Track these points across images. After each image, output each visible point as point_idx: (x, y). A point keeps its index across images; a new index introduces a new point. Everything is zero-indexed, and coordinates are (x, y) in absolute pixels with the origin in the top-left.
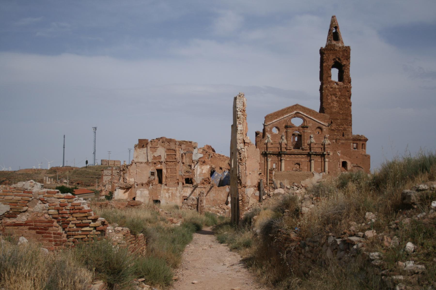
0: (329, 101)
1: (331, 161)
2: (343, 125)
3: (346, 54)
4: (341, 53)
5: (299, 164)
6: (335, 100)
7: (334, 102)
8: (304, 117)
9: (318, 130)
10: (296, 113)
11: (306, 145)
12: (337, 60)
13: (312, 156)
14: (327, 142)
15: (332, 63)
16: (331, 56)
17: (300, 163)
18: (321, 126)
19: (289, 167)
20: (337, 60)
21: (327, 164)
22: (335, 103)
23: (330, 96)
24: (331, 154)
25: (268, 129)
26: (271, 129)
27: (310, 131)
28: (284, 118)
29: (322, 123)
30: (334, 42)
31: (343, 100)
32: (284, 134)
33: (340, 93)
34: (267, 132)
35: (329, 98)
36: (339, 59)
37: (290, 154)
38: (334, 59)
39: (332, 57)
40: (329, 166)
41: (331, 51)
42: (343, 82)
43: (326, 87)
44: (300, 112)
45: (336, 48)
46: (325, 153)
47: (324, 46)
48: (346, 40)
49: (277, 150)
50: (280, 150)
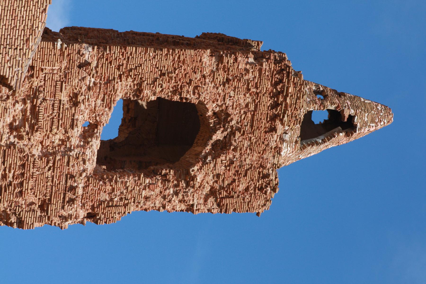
12: (218, 136)
20: (218, 136)
33: (37, 152)
36: (222, 147)
38: (222, 117)
39: (238, 100)
41: (267, 101)
42: (97, 175)
43: (85, 65)
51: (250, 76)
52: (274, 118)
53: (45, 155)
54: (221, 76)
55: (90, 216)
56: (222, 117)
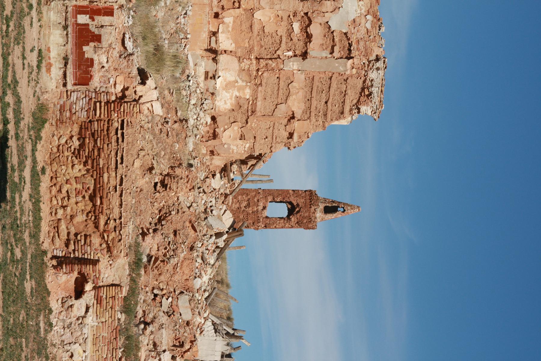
0: (240, 197)
3: (305, 221)
4: (307, 214)
6: (242, 206)
7: (238, 203)
12: (297, 209)
16: (303, 200)
20: (297, 209)
22: (237, 205)
23: (247, 199)
30: (322, 206)
31: (241, 217)
33: (251, 212)
35: (244, 196)
36: (298, 212)
38: (298, 205)
45: (313, 208)
51: (303, 195)
52: (310, 205)
53: (253, 212)
54: (295, 195)
55: (265, 226)
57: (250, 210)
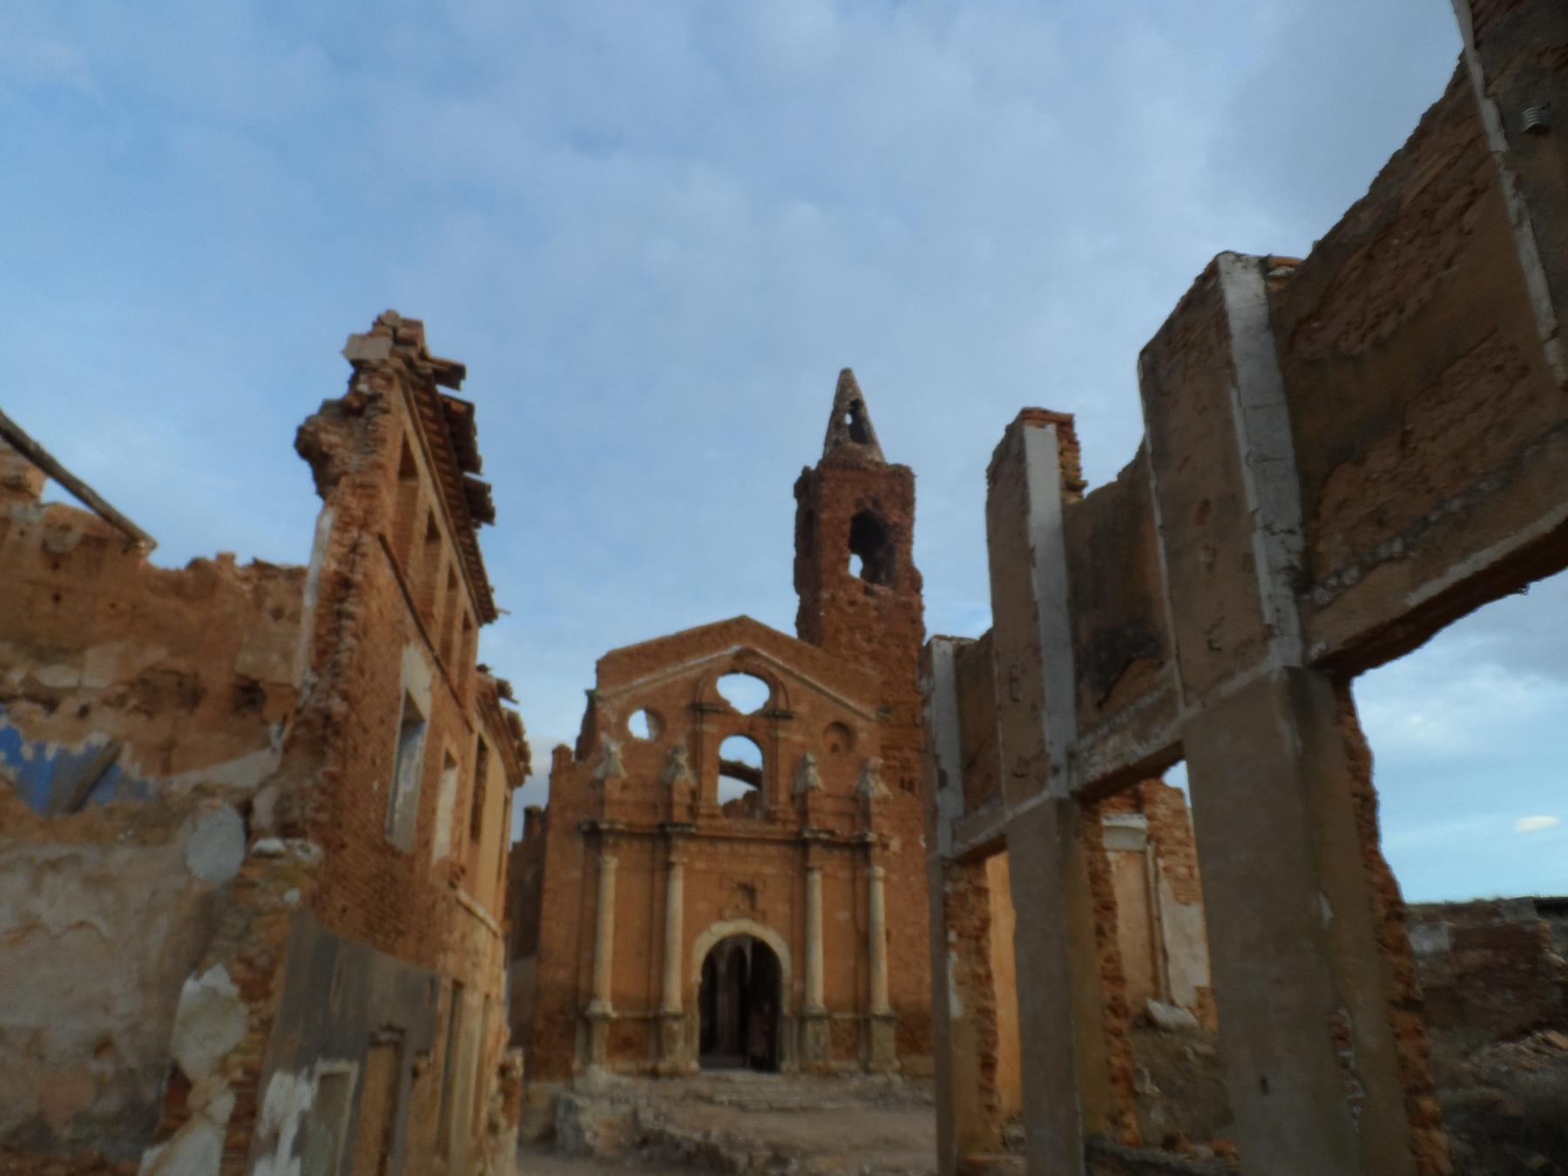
1: (895, 878)
2: (899, 749)
5: (749, 891)
8: (774, 670)
9: (834, 737)
10: (738, 656)
11: (783, 797)
12: (869, 505)
13: (815, 850)
14: (879, 788)
15: (847, 511)
17: (758, 885)
18: (847, 717)
19: (702, 906)
21: (879, 890)
24: (895, 845)
25: (608, 713)
26: (624, 715)
27: (798, 738)
28: (685, 670)
29: (851, 703)
32: (681, 741)
34: (606, 728)
36: (876, 502)
37: (713, 839)
38: (859, 503)
40: (887, 902)
42: (894, 588)
44: (759, 650)
46: (872, 837)
47: (813, 465)
48: (892, 447)
49: (645, 819)
50: (661, 819)
56: (859, 503)
57: (879, 629)
